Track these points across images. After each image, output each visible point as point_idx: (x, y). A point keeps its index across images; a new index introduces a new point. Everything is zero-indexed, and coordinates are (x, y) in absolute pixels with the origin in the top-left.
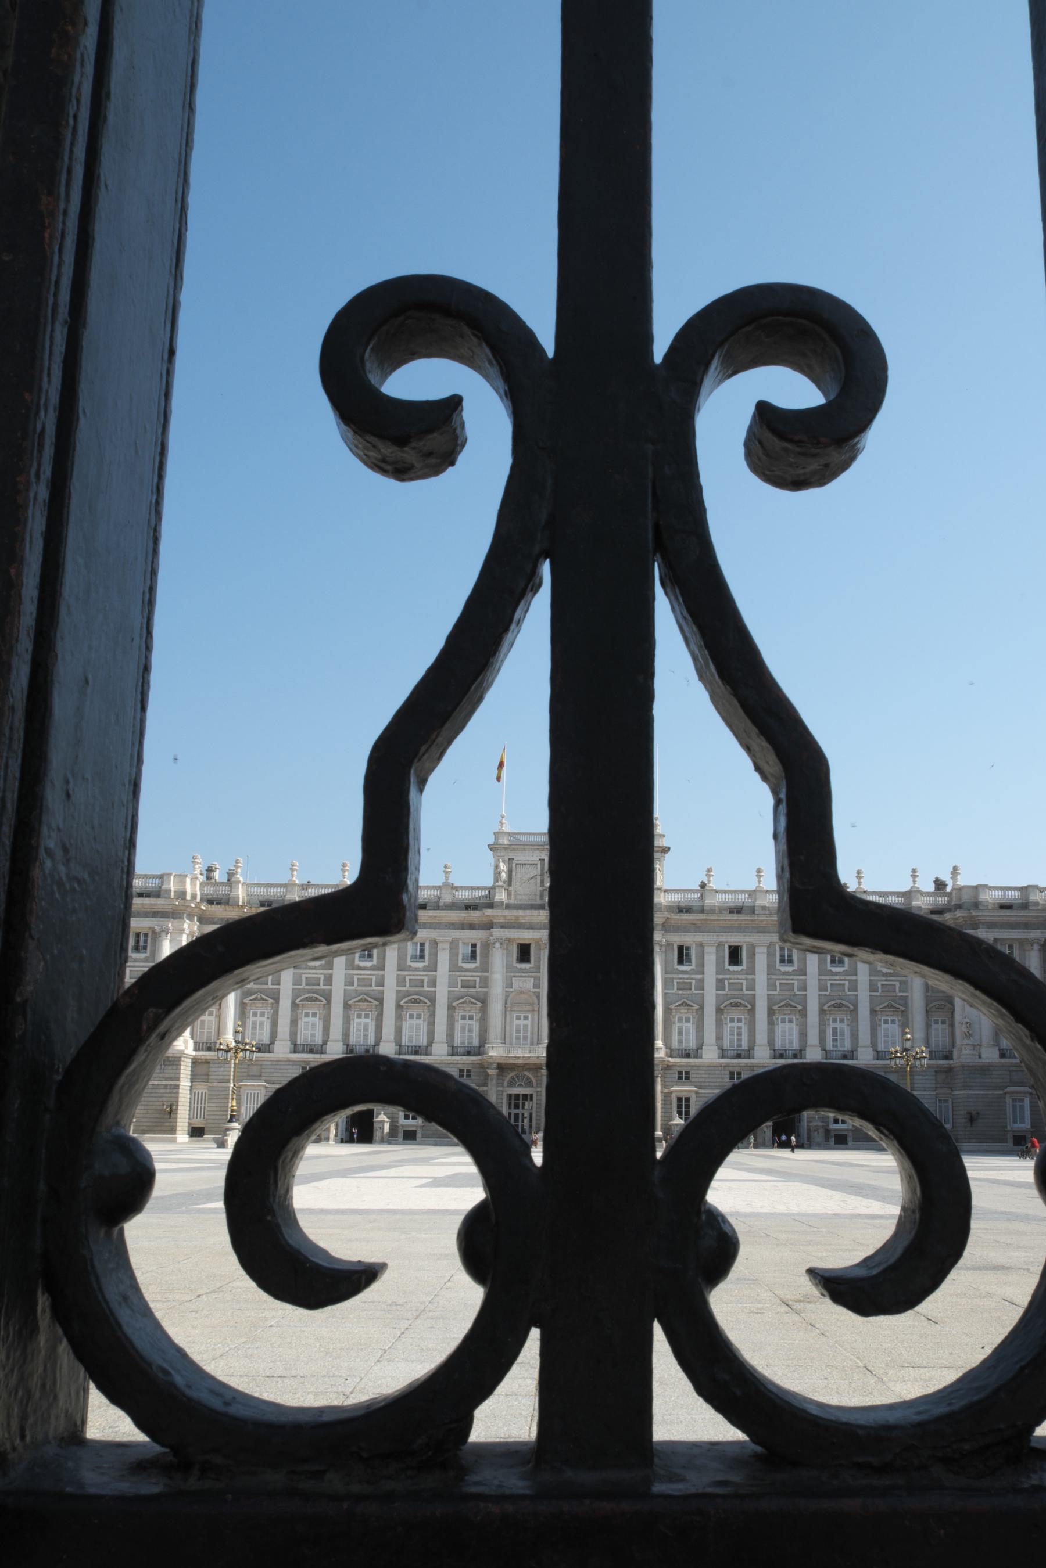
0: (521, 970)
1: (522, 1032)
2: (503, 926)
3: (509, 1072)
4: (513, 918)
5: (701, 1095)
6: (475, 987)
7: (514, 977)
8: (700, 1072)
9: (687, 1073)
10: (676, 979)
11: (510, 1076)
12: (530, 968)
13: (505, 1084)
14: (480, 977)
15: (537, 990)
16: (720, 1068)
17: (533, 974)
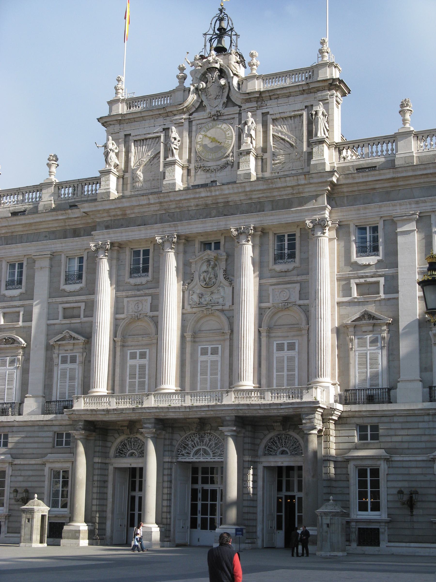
0: (137, 287)
1: (137, 376)
2: (107, 227)
3: (116, 435)
4: (119, 213)
5: (395, 464)
6: (79, 317)
7: (127, 297)
8: (393, 426)
9: (375, 428)
10: (354, 278)
11: (119, 440)
12: (148, 282)
13: (112, 452)
14: (86, 302)
15: (155, 313)
16: (426, 418)
17: (150, 291)
